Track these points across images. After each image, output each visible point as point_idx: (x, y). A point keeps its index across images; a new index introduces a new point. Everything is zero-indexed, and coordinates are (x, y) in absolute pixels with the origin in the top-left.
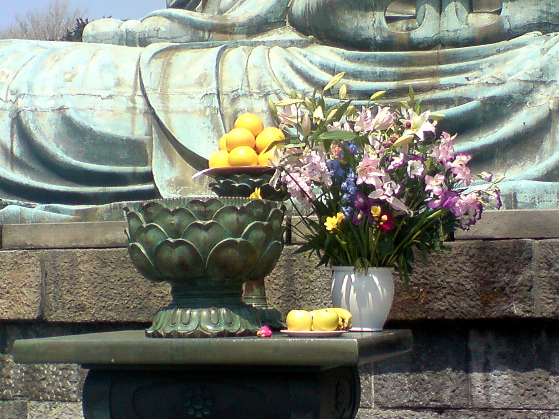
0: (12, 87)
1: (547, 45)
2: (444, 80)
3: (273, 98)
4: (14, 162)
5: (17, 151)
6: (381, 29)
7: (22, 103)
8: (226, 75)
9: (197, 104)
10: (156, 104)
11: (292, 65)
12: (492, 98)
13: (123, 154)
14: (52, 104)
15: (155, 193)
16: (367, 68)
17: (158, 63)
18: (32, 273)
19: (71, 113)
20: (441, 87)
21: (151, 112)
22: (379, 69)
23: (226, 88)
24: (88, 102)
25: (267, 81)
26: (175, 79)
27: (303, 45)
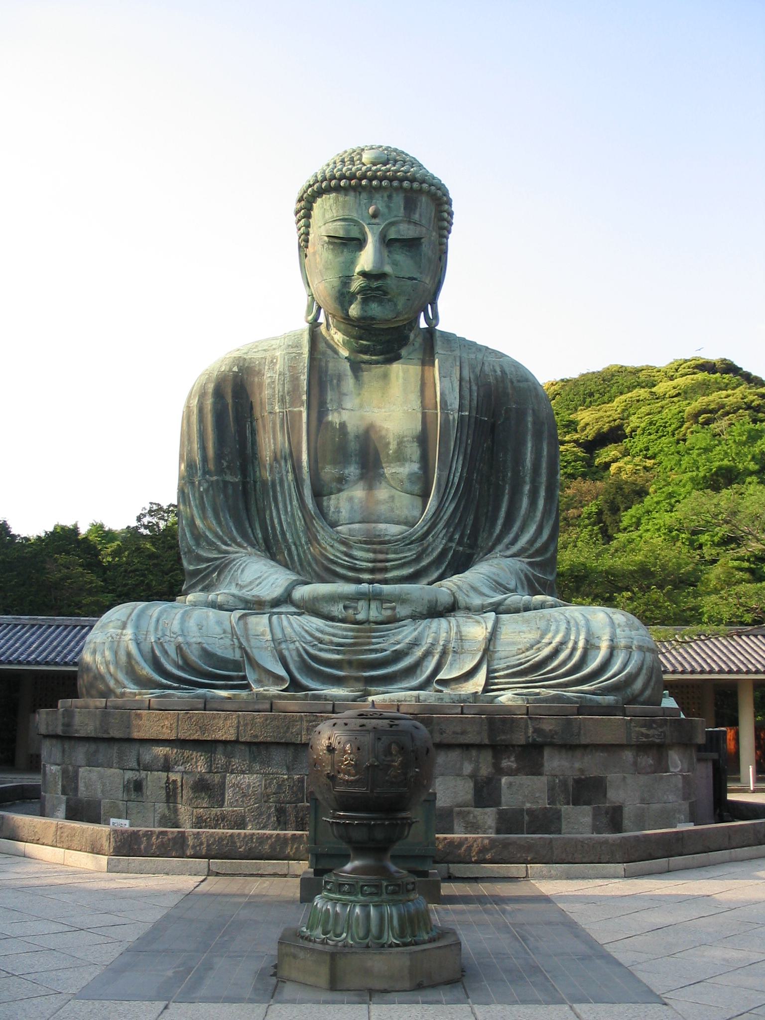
2: (374, 640)
4: (179, 667)
5: (180, 662)
7: (180, 639)
10: (245, 644)
14: (194, 640)
15: (247, 687)
16: (340, 632)
17: (241, 622)
19: (205, 645)
20: (373, 644)
21: (241, 648)
22: (345, 633)
23: (276, 637)
24: (211, 640)
26: (251, 632)
27: (300, 614)
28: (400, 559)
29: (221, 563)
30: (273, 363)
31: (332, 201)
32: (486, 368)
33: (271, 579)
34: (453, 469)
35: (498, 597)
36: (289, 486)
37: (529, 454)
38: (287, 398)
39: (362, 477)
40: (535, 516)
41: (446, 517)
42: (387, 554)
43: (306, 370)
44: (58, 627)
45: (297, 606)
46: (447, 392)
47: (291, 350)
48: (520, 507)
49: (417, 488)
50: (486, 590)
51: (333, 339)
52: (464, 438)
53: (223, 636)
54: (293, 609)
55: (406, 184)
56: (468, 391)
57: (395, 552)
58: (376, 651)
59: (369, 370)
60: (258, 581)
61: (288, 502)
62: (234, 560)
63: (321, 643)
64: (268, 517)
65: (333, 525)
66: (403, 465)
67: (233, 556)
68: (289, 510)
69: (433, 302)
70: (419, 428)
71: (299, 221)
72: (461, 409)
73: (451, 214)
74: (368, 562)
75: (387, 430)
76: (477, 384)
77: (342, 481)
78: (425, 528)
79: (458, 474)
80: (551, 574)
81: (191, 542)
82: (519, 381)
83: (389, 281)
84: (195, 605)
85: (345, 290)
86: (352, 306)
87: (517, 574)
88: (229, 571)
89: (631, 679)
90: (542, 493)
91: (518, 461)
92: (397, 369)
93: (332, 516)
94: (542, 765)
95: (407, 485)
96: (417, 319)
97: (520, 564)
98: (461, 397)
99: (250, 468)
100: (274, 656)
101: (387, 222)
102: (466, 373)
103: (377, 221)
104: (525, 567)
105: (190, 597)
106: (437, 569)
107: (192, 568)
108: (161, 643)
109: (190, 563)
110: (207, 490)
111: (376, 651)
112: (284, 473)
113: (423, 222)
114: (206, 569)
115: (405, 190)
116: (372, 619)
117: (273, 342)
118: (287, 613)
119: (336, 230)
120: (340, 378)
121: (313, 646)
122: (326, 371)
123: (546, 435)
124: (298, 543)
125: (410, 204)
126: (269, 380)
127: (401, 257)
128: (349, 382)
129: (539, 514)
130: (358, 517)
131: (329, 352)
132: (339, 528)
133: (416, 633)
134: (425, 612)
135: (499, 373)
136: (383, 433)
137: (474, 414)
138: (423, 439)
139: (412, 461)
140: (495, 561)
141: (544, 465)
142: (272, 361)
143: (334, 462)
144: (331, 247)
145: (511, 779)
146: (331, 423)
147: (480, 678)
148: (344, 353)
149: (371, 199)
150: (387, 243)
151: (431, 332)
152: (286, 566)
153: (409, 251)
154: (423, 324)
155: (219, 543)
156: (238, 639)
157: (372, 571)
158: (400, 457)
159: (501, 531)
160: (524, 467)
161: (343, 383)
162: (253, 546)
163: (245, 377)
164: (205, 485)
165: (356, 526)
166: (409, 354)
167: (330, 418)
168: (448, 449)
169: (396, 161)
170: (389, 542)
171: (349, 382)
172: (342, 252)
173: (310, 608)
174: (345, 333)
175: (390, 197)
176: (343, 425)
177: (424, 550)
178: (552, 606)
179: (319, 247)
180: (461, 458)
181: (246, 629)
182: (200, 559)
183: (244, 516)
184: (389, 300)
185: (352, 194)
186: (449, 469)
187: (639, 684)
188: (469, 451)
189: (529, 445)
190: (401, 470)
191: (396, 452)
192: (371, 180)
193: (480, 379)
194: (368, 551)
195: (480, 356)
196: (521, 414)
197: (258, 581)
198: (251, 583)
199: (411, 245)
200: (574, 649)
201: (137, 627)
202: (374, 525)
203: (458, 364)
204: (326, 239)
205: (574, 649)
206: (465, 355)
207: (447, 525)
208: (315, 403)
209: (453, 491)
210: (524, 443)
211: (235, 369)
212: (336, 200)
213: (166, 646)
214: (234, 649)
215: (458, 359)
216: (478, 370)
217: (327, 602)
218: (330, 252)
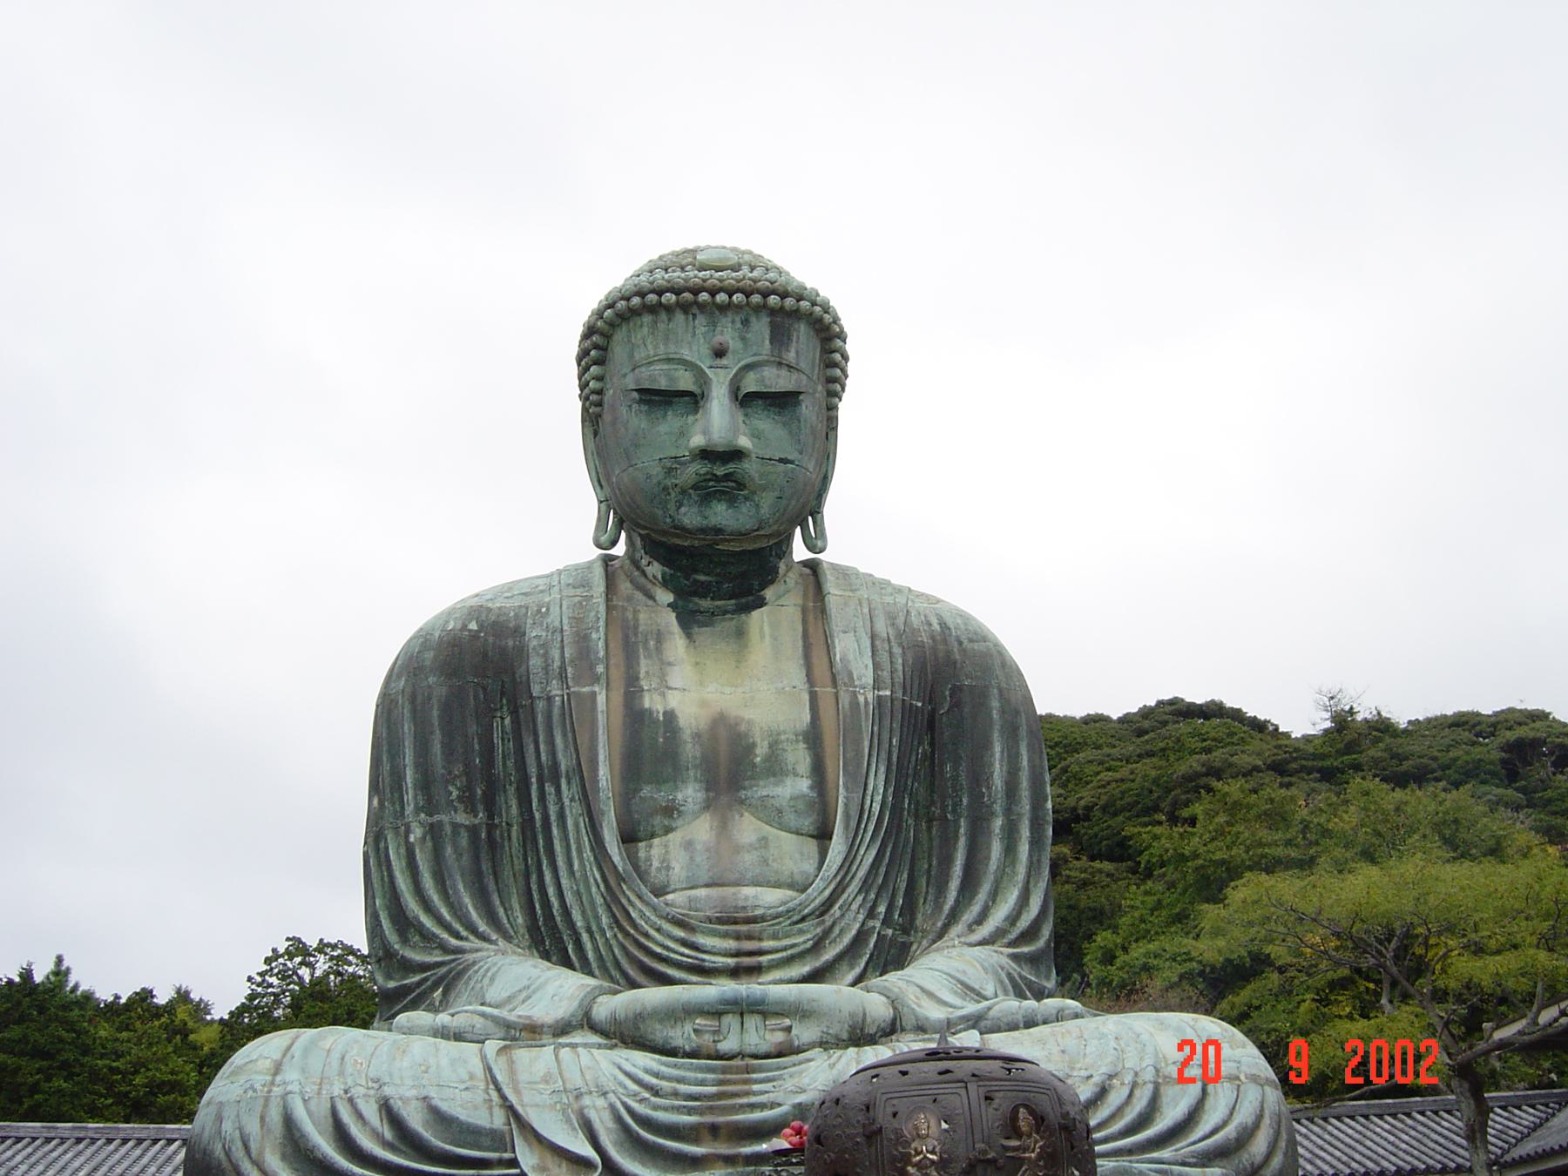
0: (371, 1075)
1: (832, 1060)
2: (755, 1087)
3: (611, 1097)
5: (388, 1135)
6: (689, 1038)
7: (387, 1091)
8: (567, 1075)
9: (546, 1098)
11: (620, 1068)
12: (800, 1104)
13: (486, 1142)
14: (413, 1092)
19: (436, 1102)
20: (755, 1093)
22: (700, 1076)
24: (447, 1093)
25: (603, 1080)
26: (523, 1077)
28: (785, 949)
29: (450, 972)
30: (541, 613)
31: (645, 330)
32: (915, 621)
33: (550, 989)
34: (870, 787)
35: (971, 1008)
36: (577, 825)
37: (997, 765)
38: (569, 670)
39: (707, 806)
40: (1015, 873)
41: (861, 873)
42: (760, 939)
43: (602, 623)
44: (125, 1141)
45: (604, 1033)
46: (851, 657)
47: (572, 592)
48: (988, 858)
49: (807, 823)
51: (644, 574)
52: (886, 736)
53: (468, 1084)
54: (596, 1039)
55: (773, 300)
56: (886, 655)
57: (775, 937)
58: (762, 1106)
60: (527, 993)
61: (574, 854)
62: (474, 963)
63: (656, 1092)
64: (534, 887)
65: (660, 892)
67: (470, 957)
68: (576, 867)
69: (816, 511)
70: (807, 717)
71: (587, 369)
72: (877, 684)
73: (846, 358)
74: (725, 955)
75: (750, 722)
76: (900, 645)
77: (671, 810)
78: (827, 893)
79: (879, 798)
80: (1048, 978)
81: (392, 937)
82: (971, 640)
83: (746, 465)
85: (669, 482)
86: (683, 510)
87: (996, 973)
88: (467, 983)
89: (1245, 1136)
90: (1025, 832)
91: (979, 777)
93: (656, 876)
95: (791, 819)
96: (789, 538)
97: (998, 956)
98: (876, 666)
99: (501, 799)
100: (568, 1121)
101: (743, 363)
102: (882, 627)
103: (724, 361)
104: (1005, 961)
105: (402, 1018)
106: (852, 967)
107: (392, 984)
108: (351, 1100)
109: (389, 977)
110: (424, 838)
111: (762, 1106)
112: (567, 802)
113: (803, 365)
114: (419, 984)
115: (773, 312)
116: (748, 1050)
117: (540, 582)
118: (585, 1045)
119: (652, 378)
120: (660, 637)
121: (641, 1101)
122: (636, 627)
123: (1023, 732)
124: (594, 928)
126: (534, 643)
127: (766, 423)
128: (677, 644)
129: (1021, 870)
130: (704, 877)
131: (639, 595)
132: (670, 897)
133: (835, 1071)
134: (845, 1036)
135: (936, 627)
136: (743, 728)
137: (899, 694)
138: (813, 738)
139: (796, 775)
140: (954, 952)
141: (1025, 783)
142: (539, 611)
143: (659, 780)
144: (644, 408)
146: (650, 711)
148: (665, 597)
149: (713, 324)
150: (745, 400)
151: (813, 567)
153: (780, 414)
154: (800, 552)
155: (445, 936)
156: (499, 1089)
157: (735, 973)
158: (775, 768)
159: (957, 901)
160: (989, 788)
161: (666, 645)
162: (508, 938)
163: (491, 639)
165: (702, 892)
166: (779, 597)
167: (647, 705)
168: (859, 752)
169: (752, 269)
170: (763, 919)
172: (665, 415)
174: (665, 561)
175: (746, 322)
176: (670, 716)
178: (1077, 1016)
179: (624, 410)
180: (882, 769)
181: (512, 1072)
182: (408, 967)
183: (492, 886)
184: (746, 499)
185: (680, 317)
187: (1259, 1145)
188: (895, 759)
189: (997, 748)
191: (767, 759)
192: (713, 293)
193: (905, 635)
194: (725, 935)
195: (901, 600)
196: (981, 695)
197: (527, 993)
198: (509, 999)
199: (782, 402)
201: (303, 1071)
202: (732, 890)
203: (866, 610)
204: (635, 395)
205: (1134, 1085)
206: (876, 597)
207: (865, 887)
208: (617, 675)
209: (871, 827)
210: (986, 745)
211: (473, 626)
214: (491, 1108)
215: (865, 605)
216: (900, 621)
217: (661, 1021)
218: (643, 417)
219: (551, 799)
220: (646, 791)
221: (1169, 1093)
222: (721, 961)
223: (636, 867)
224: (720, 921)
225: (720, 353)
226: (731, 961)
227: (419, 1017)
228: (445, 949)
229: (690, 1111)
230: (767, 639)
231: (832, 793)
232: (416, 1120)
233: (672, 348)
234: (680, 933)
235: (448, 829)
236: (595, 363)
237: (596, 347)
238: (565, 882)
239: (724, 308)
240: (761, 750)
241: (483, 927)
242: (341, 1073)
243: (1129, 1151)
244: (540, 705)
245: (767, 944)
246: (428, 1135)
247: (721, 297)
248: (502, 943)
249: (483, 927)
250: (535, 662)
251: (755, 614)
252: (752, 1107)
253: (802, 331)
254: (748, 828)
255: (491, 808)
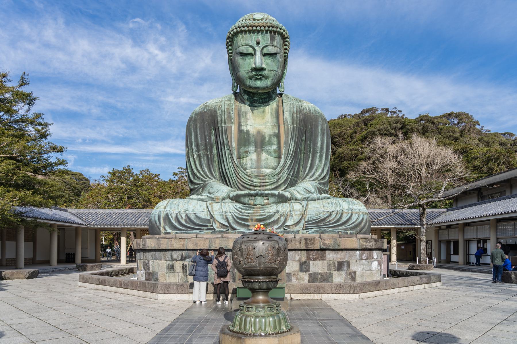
7: (187, 212)
18: (207, 241)
26: (214, 209)
35: (308, 195)
39: (256, 151)
41: (287, 166)
46: (288, 117)
49: (276, 155)
50: (303, 193)
54: (231, 201)
57: (268, 179)
58: (262, 215)
59: (257, 110)
66: (271, 146)
67: (207, 182)
70: (277, 132)
72: (293, 124)
75: (265, 133)
77: (247, 152)
79: (292, 150)
84: (193, 199)
85: (247, 76)
92: (268, 109)
94: (325, 256)
95: (273, 154)
100: (223, 218)
105: (191, 197)
111: (262, 215)
113: (278, 46)
115: (271, 32)
119: (242, 50)
120: (246, 113)
125: (272, 39)
130: (254, 166)
136: (263, 134)
143: (245, 146)
145: (314, 262)
147: (301, 225)
152: (228, 185)
155: (202, 178)
157: (260, 186)
158: (270, 143)
164: (196, 156)
168: (288, 140)
171: (250, 115)
173: (236, 199)
176: (248, 131)
177: (279, 179)
178: (328, 198)
186: (288, 147)
190: (270, 148)
191: (268, 141)
193: (300, 111)
194: (258, 179)
200: (337, 214)
207: (288, 169)
211: (206, 110)
212: (243, 37)
213: (182, 215)
219: (223, 149)
220: (243, 148)
221: (344, 215)
222: (257, 184)
223: (240, 164)
224: (257, 176)
225: (258, 43)
226: (259, 184)
227: (194, 197)
228: (202, 180)
229: (247, 216)
230: (270, 114)
231: (282, 149)
232: (192, 217)
233: (247, 42)
234: (249, 178)
235: (202, 155)
236: (230, 45)
237: (230, 41)
238: (226, 167)
239: (258, 32)
240: (267, 139)
241: (210, 176)
242: (178, 209)
243: (334, 227)
244: (220, 128)
245: (267, 181)
246: (195, 221)
247: (258, 28)
248: (214, 179)
249: (210, 176)
250: (219, 119)
251: (267, 107)
252: (260, 215)
253: (278, 38)
254: (264, 156)
255: (211, 151)
